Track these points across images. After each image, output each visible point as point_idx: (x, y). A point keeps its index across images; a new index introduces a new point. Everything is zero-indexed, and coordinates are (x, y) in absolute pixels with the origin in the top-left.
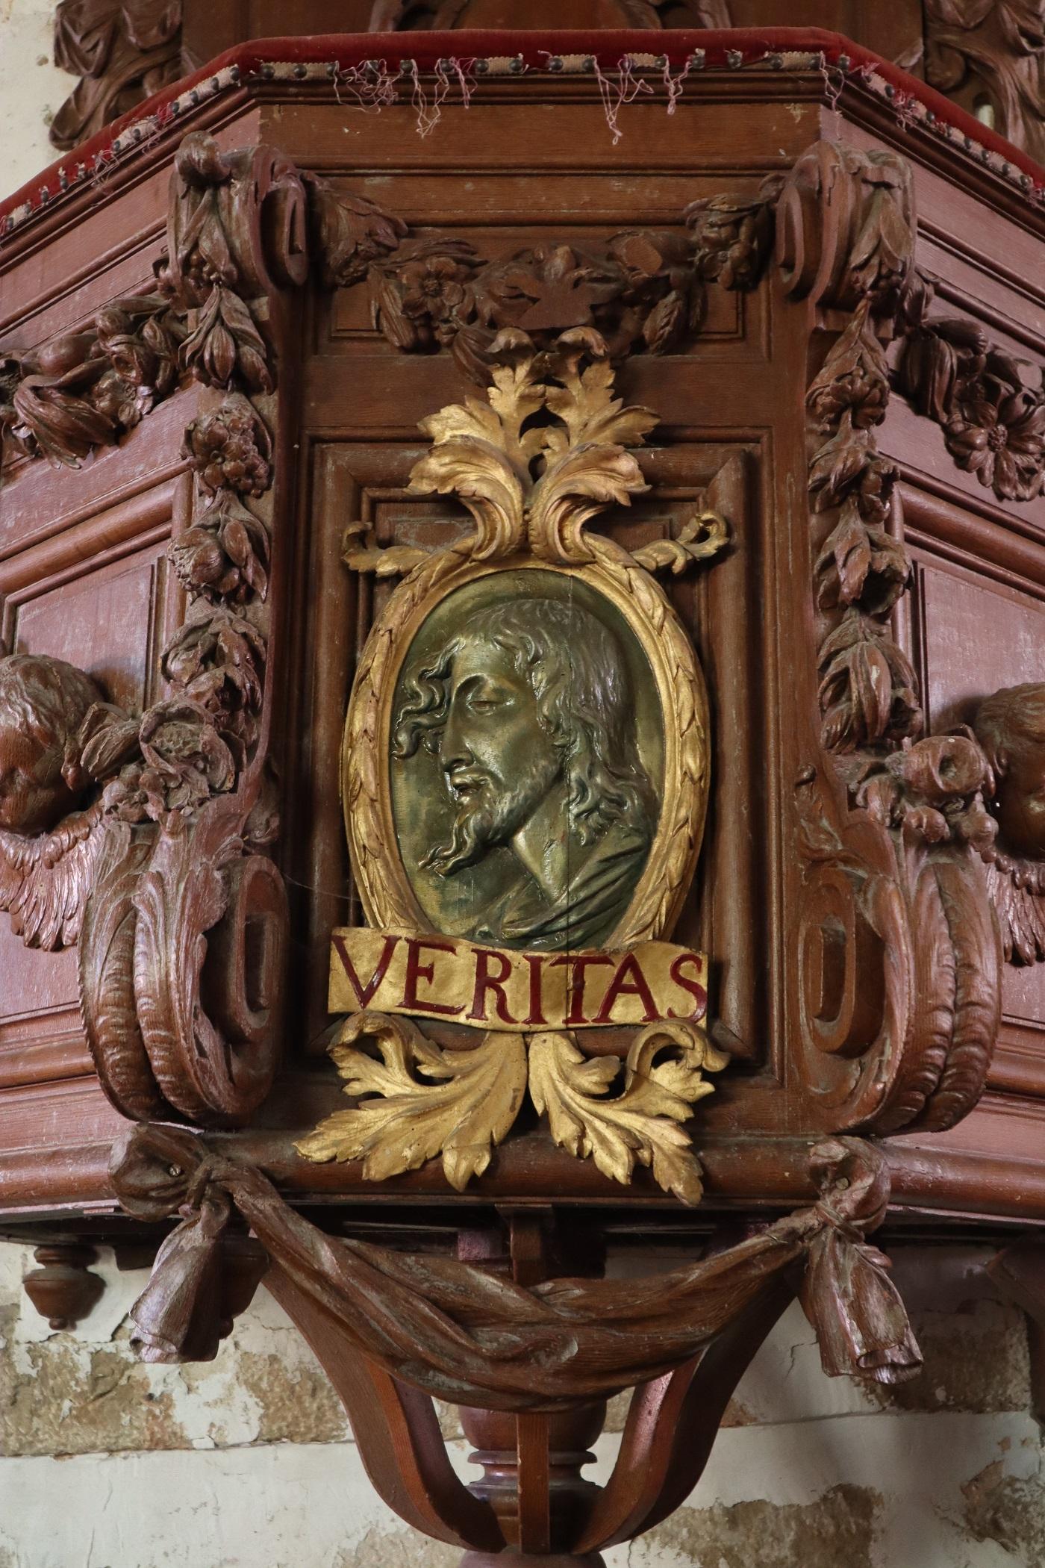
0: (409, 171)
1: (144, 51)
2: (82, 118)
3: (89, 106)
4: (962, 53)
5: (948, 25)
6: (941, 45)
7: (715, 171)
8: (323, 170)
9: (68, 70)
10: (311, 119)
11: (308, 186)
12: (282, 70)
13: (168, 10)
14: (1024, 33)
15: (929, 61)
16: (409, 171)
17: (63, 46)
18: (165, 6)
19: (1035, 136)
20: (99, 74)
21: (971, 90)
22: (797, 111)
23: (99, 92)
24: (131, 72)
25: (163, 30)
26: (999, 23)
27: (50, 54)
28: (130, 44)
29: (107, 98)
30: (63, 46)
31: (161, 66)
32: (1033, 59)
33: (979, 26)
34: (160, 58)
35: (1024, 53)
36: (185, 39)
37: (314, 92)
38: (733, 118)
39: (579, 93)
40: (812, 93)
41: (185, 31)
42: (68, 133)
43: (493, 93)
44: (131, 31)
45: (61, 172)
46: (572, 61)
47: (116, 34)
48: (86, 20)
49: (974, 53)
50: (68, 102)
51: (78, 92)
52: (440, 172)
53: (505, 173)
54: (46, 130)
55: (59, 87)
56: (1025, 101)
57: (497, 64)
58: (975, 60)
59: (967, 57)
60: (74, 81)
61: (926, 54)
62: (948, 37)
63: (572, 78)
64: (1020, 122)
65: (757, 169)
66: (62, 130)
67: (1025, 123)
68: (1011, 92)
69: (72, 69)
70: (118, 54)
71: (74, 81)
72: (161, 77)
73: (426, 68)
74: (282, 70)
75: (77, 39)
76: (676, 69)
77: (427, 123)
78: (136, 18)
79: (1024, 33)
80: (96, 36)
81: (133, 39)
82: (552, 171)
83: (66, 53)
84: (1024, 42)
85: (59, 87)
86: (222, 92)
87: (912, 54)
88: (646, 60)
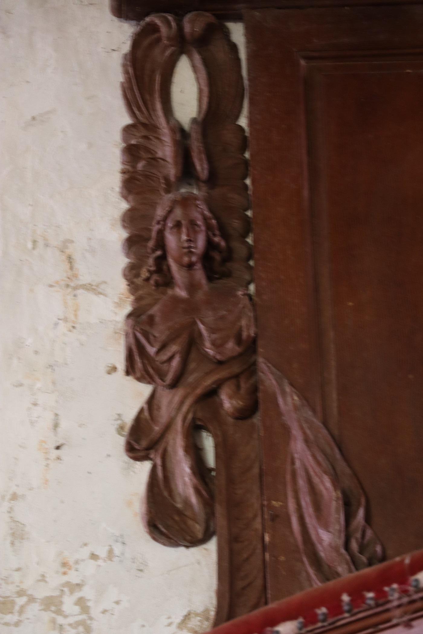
1: (220, 363)
2: (157, 429)
3: (164, 414)
9: (139, 379)
13: (244, 322)
17: (137, 359)
18: (239, 318)
20: (174, 385)
24: (209, 382)
25: (239, 340)
27: (121, 364)
28: (206, 356)
29: (185, 408)
30: (137, 359)
31: (236, 377)
34: (236, 369)
36: (260, 350)
41: (260, 343)
42: (144, 443)
44: (208, 344)
45: (346, 598)
47: (193, 343)
48: (160, 332)
50: (141, 411)
51: (151, 401)
54: (121, 441)
55: (132, 396)
60: (146, 390)
66: (137, 441)
69: (145, 377)
70: (192, 365)
71: (146, 390)
72: (238, 387)
75: (152, 350)
78: (212, 330)
80: (174, 348)
81: (211, 352)
83: (138, 363)
85: (132, 396)
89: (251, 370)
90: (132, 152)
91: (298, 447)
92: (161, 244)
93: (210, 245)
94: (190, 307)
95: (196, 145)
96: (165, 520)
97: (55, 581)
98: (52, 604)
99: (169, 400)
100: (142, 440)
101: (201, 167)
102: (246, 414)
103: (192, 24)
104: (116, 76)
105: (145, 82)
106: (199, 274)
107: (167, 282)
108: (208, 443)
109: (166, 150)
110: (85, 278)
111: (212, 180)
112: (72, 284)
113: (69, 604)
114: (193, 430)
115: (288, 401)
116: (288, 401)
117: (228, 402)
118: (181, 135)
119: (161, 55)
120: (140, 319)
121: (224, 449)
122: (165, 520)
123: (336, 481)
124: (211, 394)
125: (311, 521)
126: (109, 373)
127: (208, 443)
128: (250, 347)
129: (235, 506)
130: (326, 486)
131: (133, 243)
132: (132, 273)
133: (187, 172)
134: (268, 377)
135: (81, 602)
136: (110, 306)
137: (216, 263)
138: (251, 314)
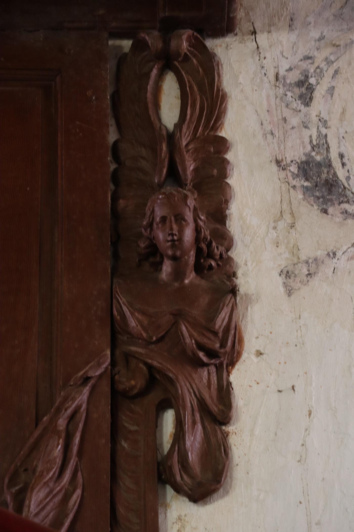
4: (146, 364)
5: (133, 338)
6: (128, 356)
14: (201, 347)
15: (116, 369)
19: (213, 440)
21: (155, 397)
26: (179, 337)
32: (213, 369)
33: (160, 340)
35: (203, 365)
49: (155, 364)
56: (203, 406)
58: (159, 371)
59: (150, 367)
61: (113, 363)
62: (133, 348)
64: (199, 427)
67: (204, 427)
68: (189, 400)
79: (201, 347)
84: (201, 354)
87: (99, 365)
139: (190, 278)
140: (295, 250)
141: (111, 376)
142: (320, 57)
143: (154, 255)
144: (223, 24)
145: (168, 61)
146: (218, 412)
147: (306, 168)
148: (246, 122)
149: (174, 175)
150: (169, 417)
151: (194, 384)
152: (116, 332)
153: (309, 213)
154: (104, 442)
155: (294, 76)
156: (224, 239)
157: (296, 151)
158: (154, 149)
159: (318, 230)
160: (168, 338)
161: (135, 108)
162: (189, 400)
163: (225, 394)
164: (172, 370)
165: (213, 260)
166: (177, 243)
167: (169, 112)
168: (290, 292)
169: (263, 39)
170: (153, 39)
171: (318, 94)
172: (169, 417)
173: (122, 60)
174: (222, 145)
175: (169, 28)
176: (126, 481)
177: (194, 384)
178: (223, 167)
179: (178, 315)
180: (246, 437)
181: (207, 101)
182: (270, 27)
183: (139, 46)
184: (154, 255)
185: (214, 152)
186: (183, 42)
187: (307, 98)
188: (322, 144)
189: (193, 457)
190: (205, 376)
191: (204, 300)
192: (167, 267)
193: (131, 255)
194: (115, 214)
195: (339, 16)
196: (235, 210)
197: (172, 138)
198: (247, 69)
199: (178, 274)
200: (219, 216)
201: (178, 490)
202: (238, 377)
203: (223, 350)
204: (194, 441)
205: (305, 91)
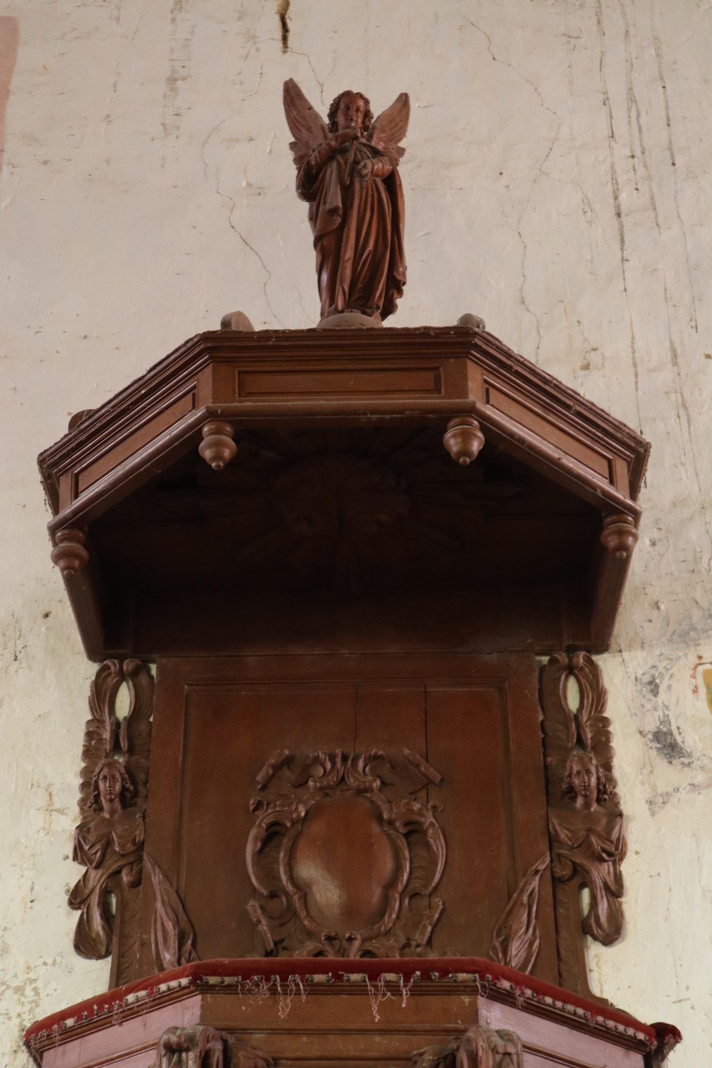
0: (274, 1031)
1: (123, 856)
2: (87, 892)
3: (91, 884)
4: (571, 861)
6: (560, 856)
7: (426, 1032)
8: (230, 1030)
9: (80, 863)
10: (225, 1001)
11: (225, 1042)
12: (213, 980)
13: (137, 833)
14: (604, 850)
15: (554, 864)
16: (274, 1031)
17: (79, 853)
18: (136, 830)
19: (613, 907)
20: (97, 867)
21: (576, 881)
22: (467, 999)
23: (97, 878)
24: (115, 867)
25: (134, 842)
26: (590, 845)
27: (71, 855)
28: (115, 851)
29: (101, 881)
30: (79, 853)
31: (132, 863)
32: (610, 863)
33: (579, 846)
34: (131, 859)
35: (605, 861)
36: (146, 849)
37: (230, 989)
38: (435, 1002)
39: (359, 990)
40: (472, 991)
41: (146, 844)
42: (78, 900)
43: (315, 990)
44: (116, 844)
45: (95, 1007)
46: (355, 977)
47: (108, 844)
48: (92, 837)
49: (577, 861)
50: (79, 881)
52: (290, 1032)
53: (324, 1032)
54: (66, 898)
55: (74, 872)
56: (606, 886)
57: (319, 978)
58: (579, 865)
59: (574, 863)
60: (83, 869)
61: (551, 861)
62: (562, 851)
63: (355, 984)
64: (605, 899)
65: (447, 1031)
66: (75, 898)
67: (608, 900)
68: (599, 883)
69: (83, 863)
70: (108, 857)
71: (83, 869)
72: (132, 870)
73: (284, 979)
74: (213, 980)
75: (86, 847)
76: (407, 979)
77: (284, 1007)
78: (119, 837)
79: (604, 850)
80: (98, 847)
81: (117, 849)
82: (346, 1032)
83: (79, 854)
84: (604, 855)
85: (74, 872)
86: (182, 988)
87: (544, 862)
88: (391, 977)
89: (140, 860)
90: (89, 735)
91: (159, 905)
92: (97, 787)
93: (124, 789)
94: (110, 823)
95: (123, 732)
96: (85, 944)
97: (22, 977)
98: (19, 990)
99: (94, 875)
100: (77, 898)
101: (124, 744)
102: (136, 884)
103: (128, 666)
104: (87, 692)
105: (102, 696)
106: (117, 804)
107: (101, 809)
108: (114, 900)
109: (107, 735)
110: (57, 805)
111: (131, 751)
112: (50, 809)
113: (29, 991)
114: (105, 894)
115: (156, 878)
116: (156, 878)
117: (125, 878)
118: (117, 724)
119: (111, 681)
120: (82, 830)
121: (122, 903)
122: (85, 944)
123: (177, 923)
124: (118, 872)
125: (161, 947)
126: (65, 859)
127: (114, 900)
128: (140, 847)
129: (123, 937)
130: (169, 926)
131: (84, 786)
132: (82, 803)
133: (116, 747)
134: (147, 864)
135: (35, 989)
136: (69, 821)
137: (127, 799)
138: (143, 828)
139: (594, 807)
140: (654, 787)
141: (551, 868)
142: (661, 666)
143: (571, 792)
144: (602, 647)
145: (571, 670)
146: (615, 890)
147: (658, 736)
148: (620, 707)
149: (580, 742)
150: (586, 893)
151: (601, 873)
152: (552, 840)
153: (661, 764)
154: (550, 910)
155: (647, 679)
156: (611, 780)
157: (651, 726)
158: (567, 726)
159: (668, 774)
160: (585, 846)
161: (551, 698)
162: (599, 883)
163: (618, 878)
164: (585, 862)
165: (606, 794)
166: (587, 787)
167: (573, 701)
168: (653, 814)
169: (626, 655)
170: (563, 658)
171: (662, 689)
172: (586, 893)
173: (542, 669)
174: (606, 722)
175: (571, 650)
176: (564, 933)
177: (601, 873)
178: (607, 736)
179: (590, 831)
180: (630, 904)
181: (595, 694)
182: (630, 647)
183: (553, 661)
184: (571, 792)
185: (602, 725)
186: (580, 658)
187: (655, 691)
188: (666, 721)
189: (603, 919)
190: (606, 868)
191: (604, 821)
192: (580, 801)
193: (559, 793)
194: (546, 767)
195: (670, 641)
196: (616, 762)
197: (577, 717)
198: (617, 672)
199: (587, 805)
200: (608, 767)
201: (595, 938)
202: (625, 867)
203: (615, 852)
204: (603, 908)
205: (654, 687)
